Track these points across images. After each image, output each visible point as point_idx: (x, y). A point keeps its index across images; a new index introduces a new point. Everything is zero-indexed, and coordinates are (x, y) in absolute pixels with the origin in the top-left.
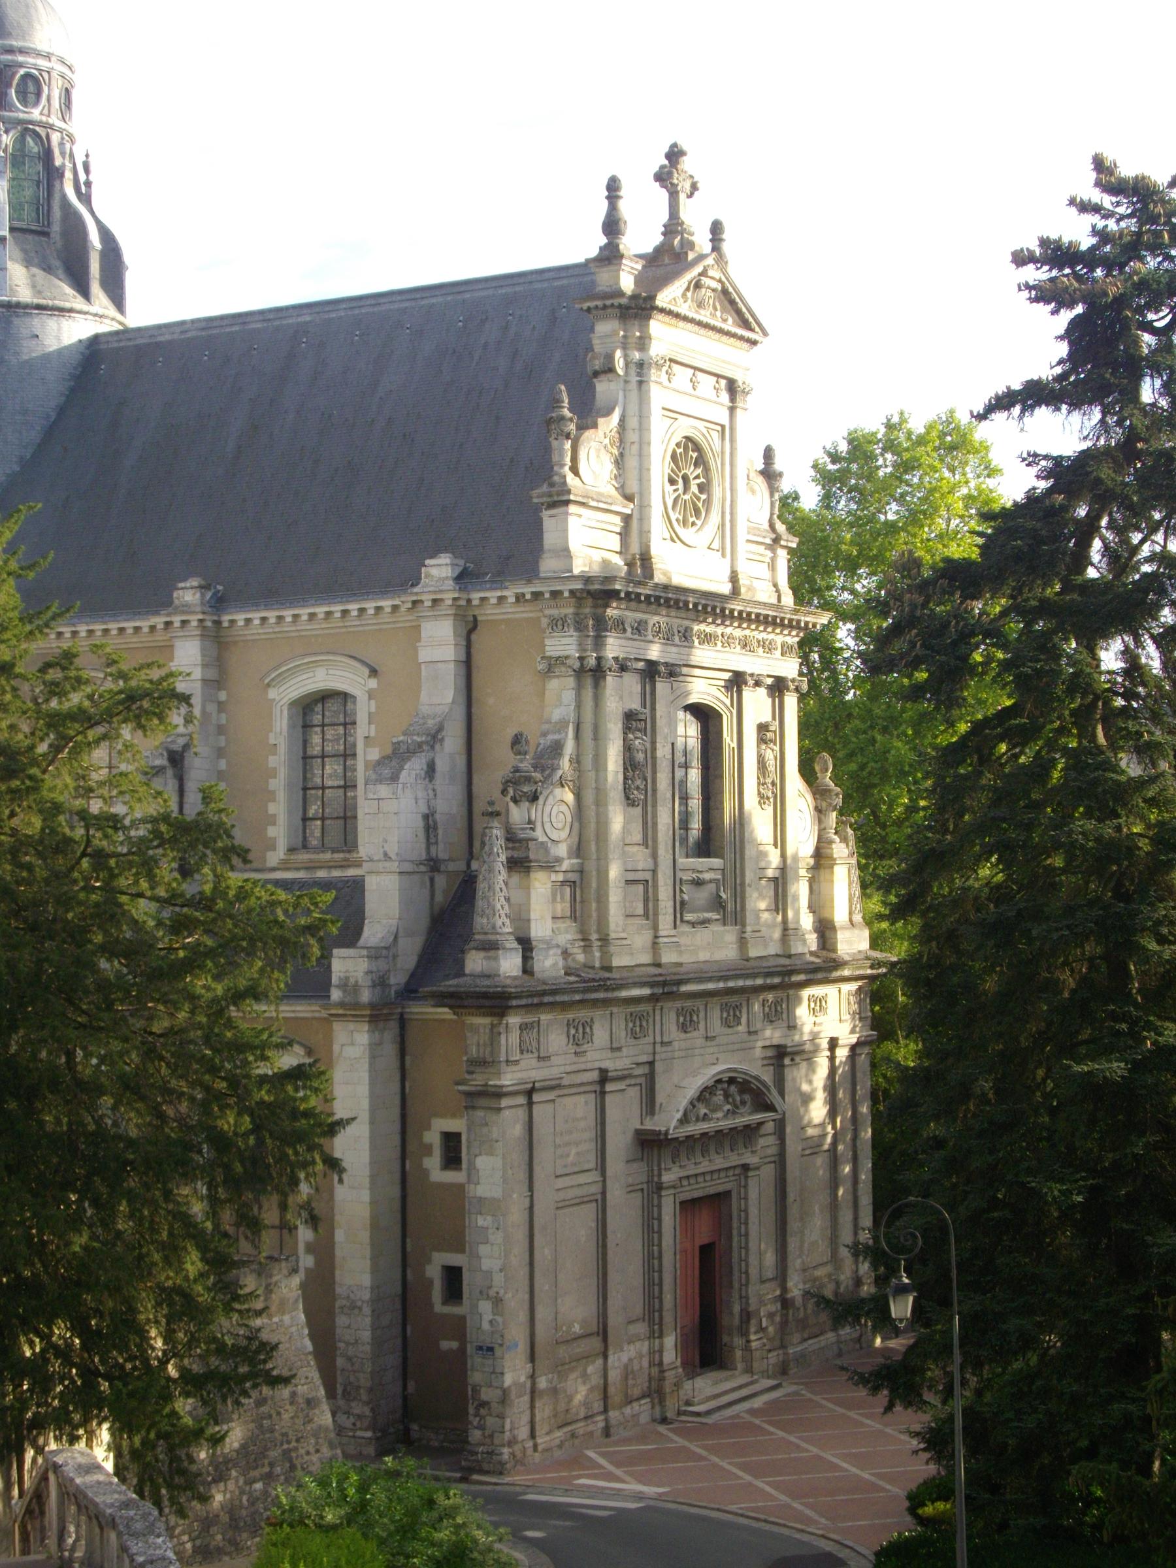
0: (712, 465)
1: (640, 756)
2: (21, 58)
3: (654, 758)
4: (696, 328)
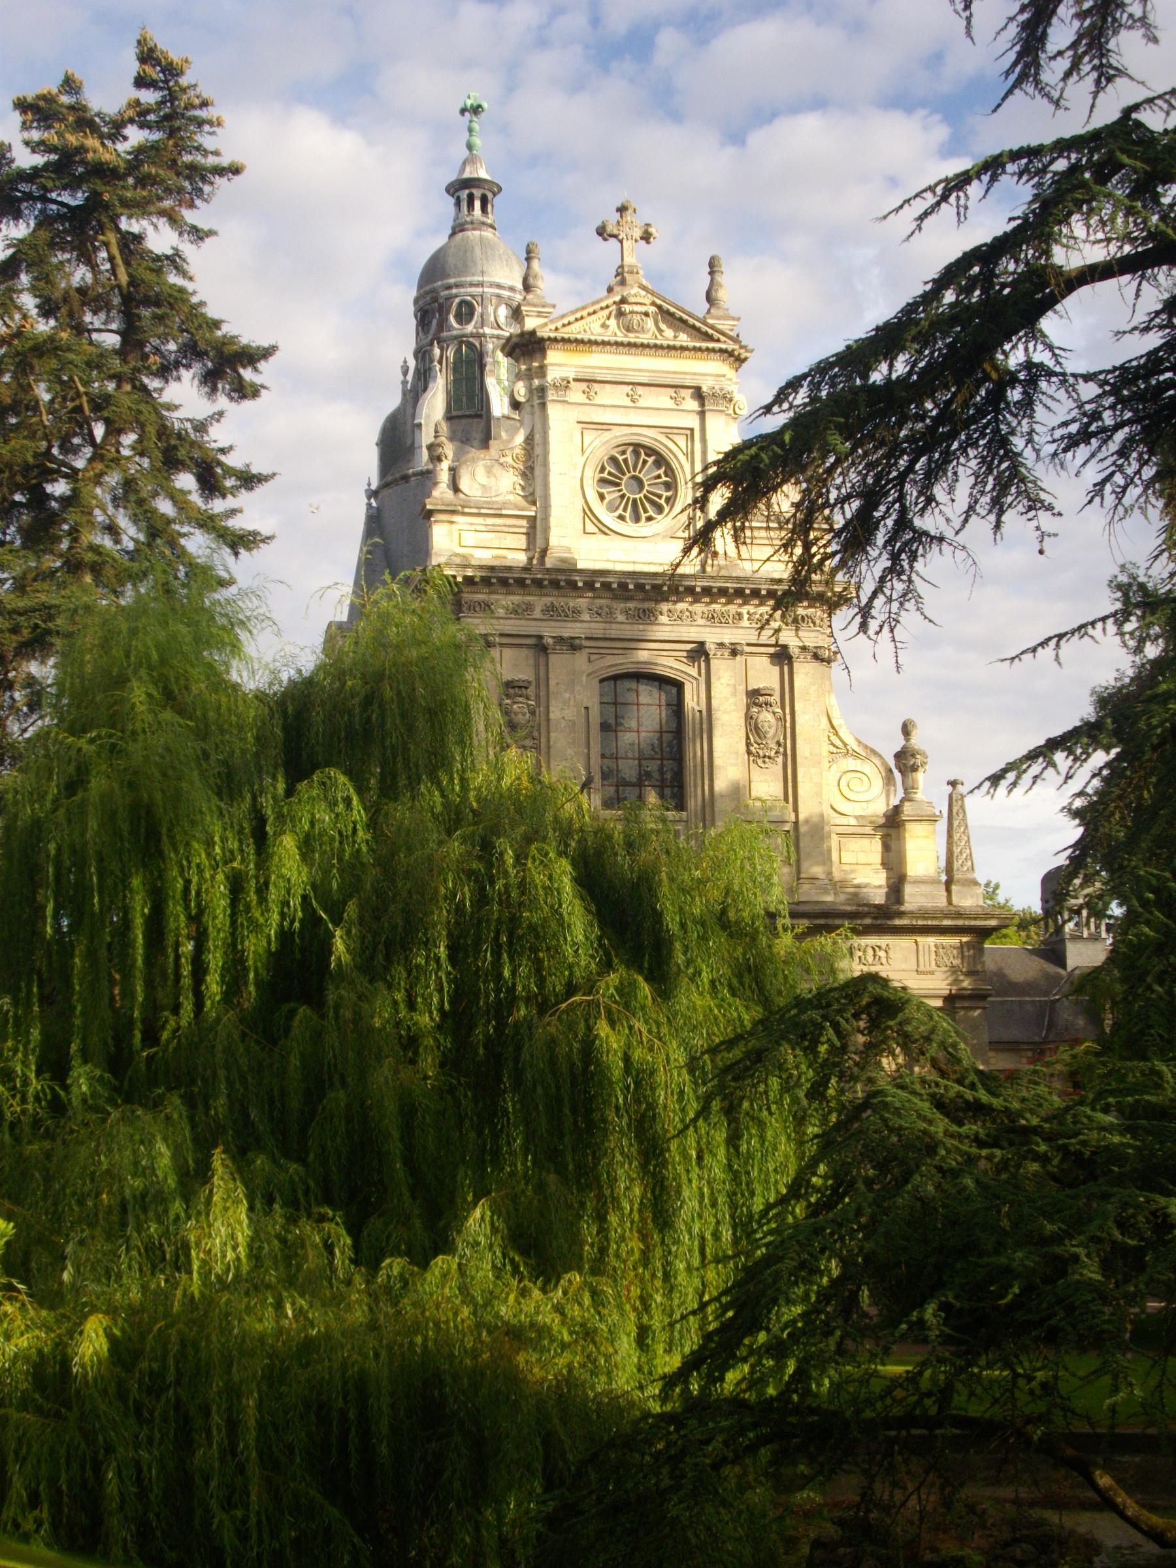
0: (674, 464)
1: (520, 719)
2: (454, 291)
3: (548, 720)
4: (626, 350)
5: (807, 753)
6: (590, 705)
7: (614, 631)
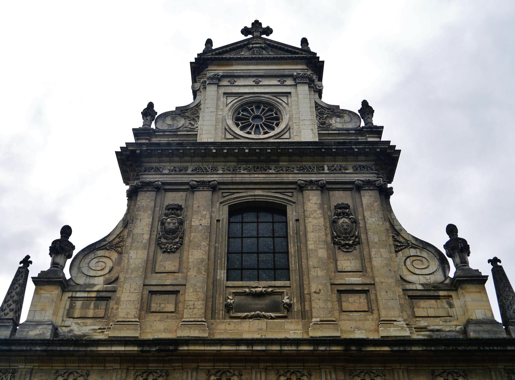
0: (281, 108)
5: (376, 240)
6: (221, 219)
7: (238, 178)
